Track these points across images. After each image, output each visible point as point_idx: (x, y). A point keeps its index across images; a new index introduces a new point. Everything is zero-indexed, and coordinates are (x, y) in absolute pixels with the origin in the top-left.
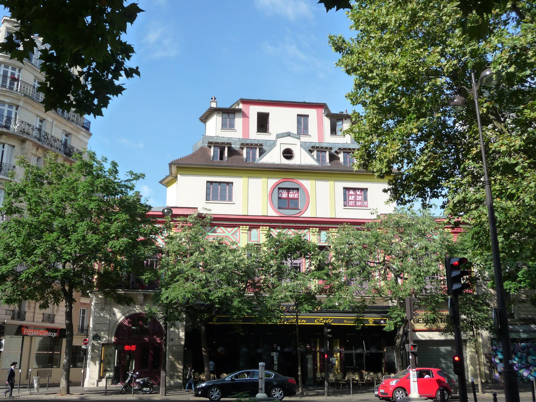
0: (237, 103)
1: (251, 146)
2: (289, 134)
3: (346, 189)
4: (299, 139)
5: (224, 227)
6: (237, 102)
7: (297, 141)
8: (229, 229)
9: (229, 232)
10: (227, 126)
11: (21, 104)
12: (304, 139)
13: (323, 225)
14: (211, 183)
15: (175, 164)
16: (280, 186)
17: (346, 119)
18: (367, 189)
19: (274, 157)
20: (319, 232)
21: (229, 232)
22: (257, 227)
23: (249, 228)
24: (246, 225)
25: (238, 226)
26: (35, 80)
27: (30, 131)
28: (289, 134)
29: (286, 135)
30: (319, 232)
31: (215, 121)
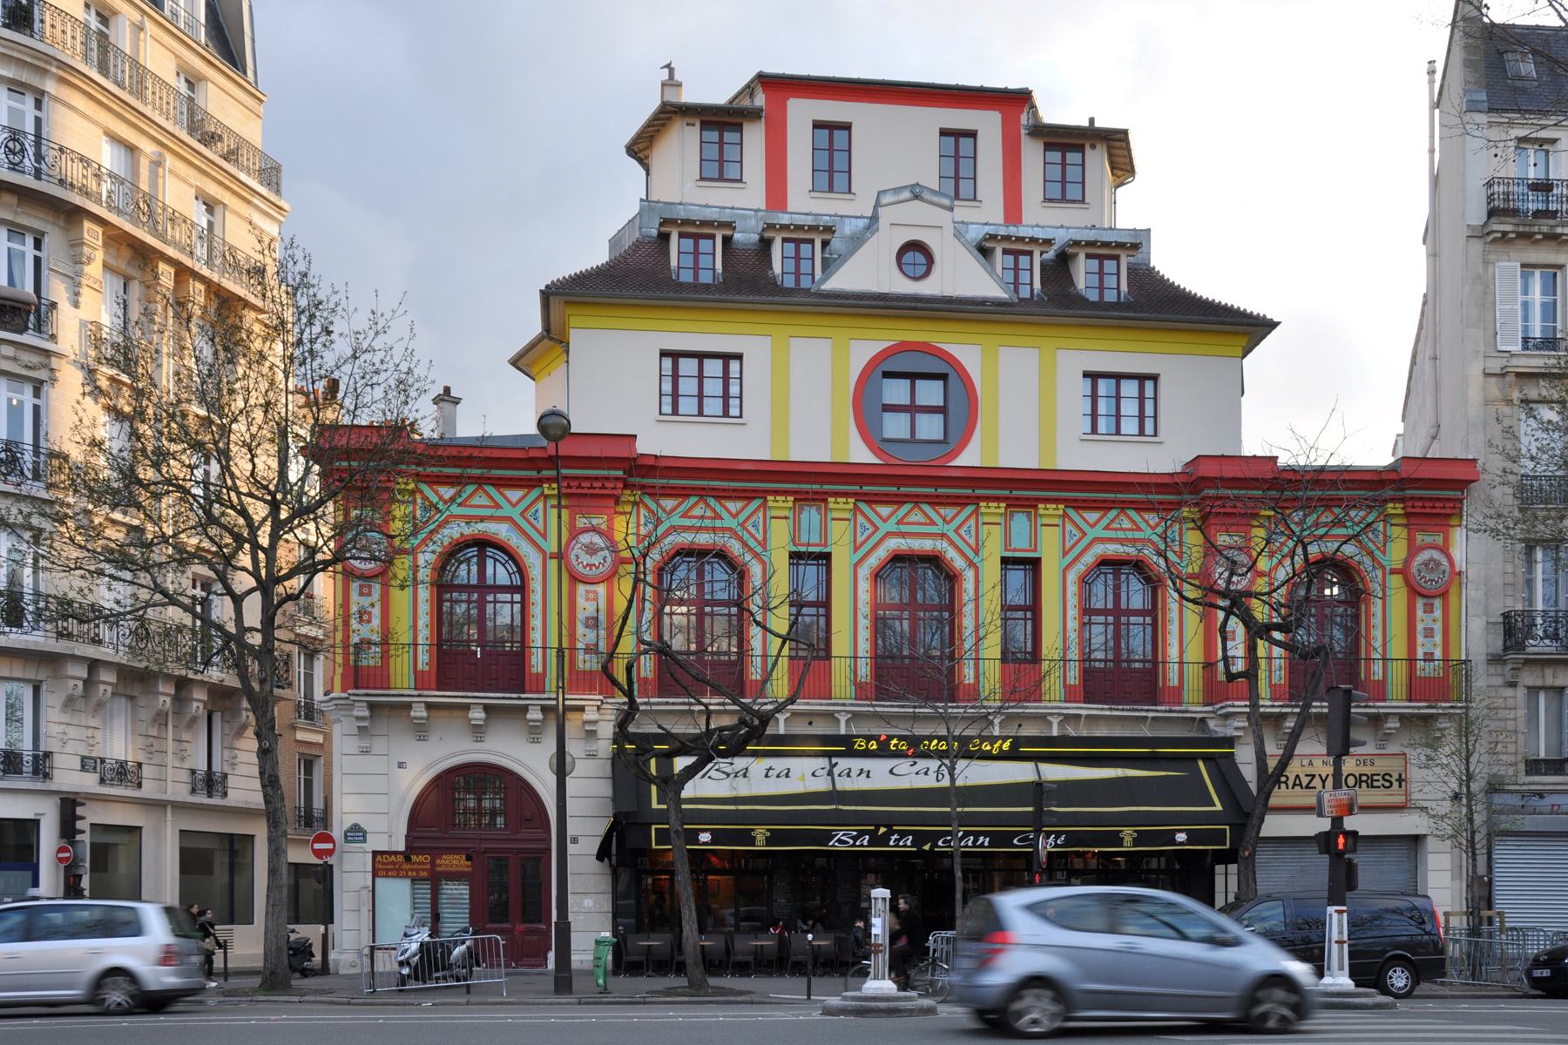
0: (749, 90)
1: (799, 235)
2: (917, 193)
3: (1093, 376)
4: (951, 209)
5: (717, 498)
6: (748, 86)
7: (943, 217)
10: (719, 170)
12: (963, 212)
13: (1023, 490)
14: (675, 355)
15: (557, 294)
16: (889, 366)
19: (869, 270)
20: (1008, 517)
21: (735, 516)
23: (796, 500)
24: (785, 493)
25: (762, 494)
26: (87, 6)
27: (92, 184)
28: (917, 193)
29: (906, 194)
30: (1008, 517)
31: (683, 144)
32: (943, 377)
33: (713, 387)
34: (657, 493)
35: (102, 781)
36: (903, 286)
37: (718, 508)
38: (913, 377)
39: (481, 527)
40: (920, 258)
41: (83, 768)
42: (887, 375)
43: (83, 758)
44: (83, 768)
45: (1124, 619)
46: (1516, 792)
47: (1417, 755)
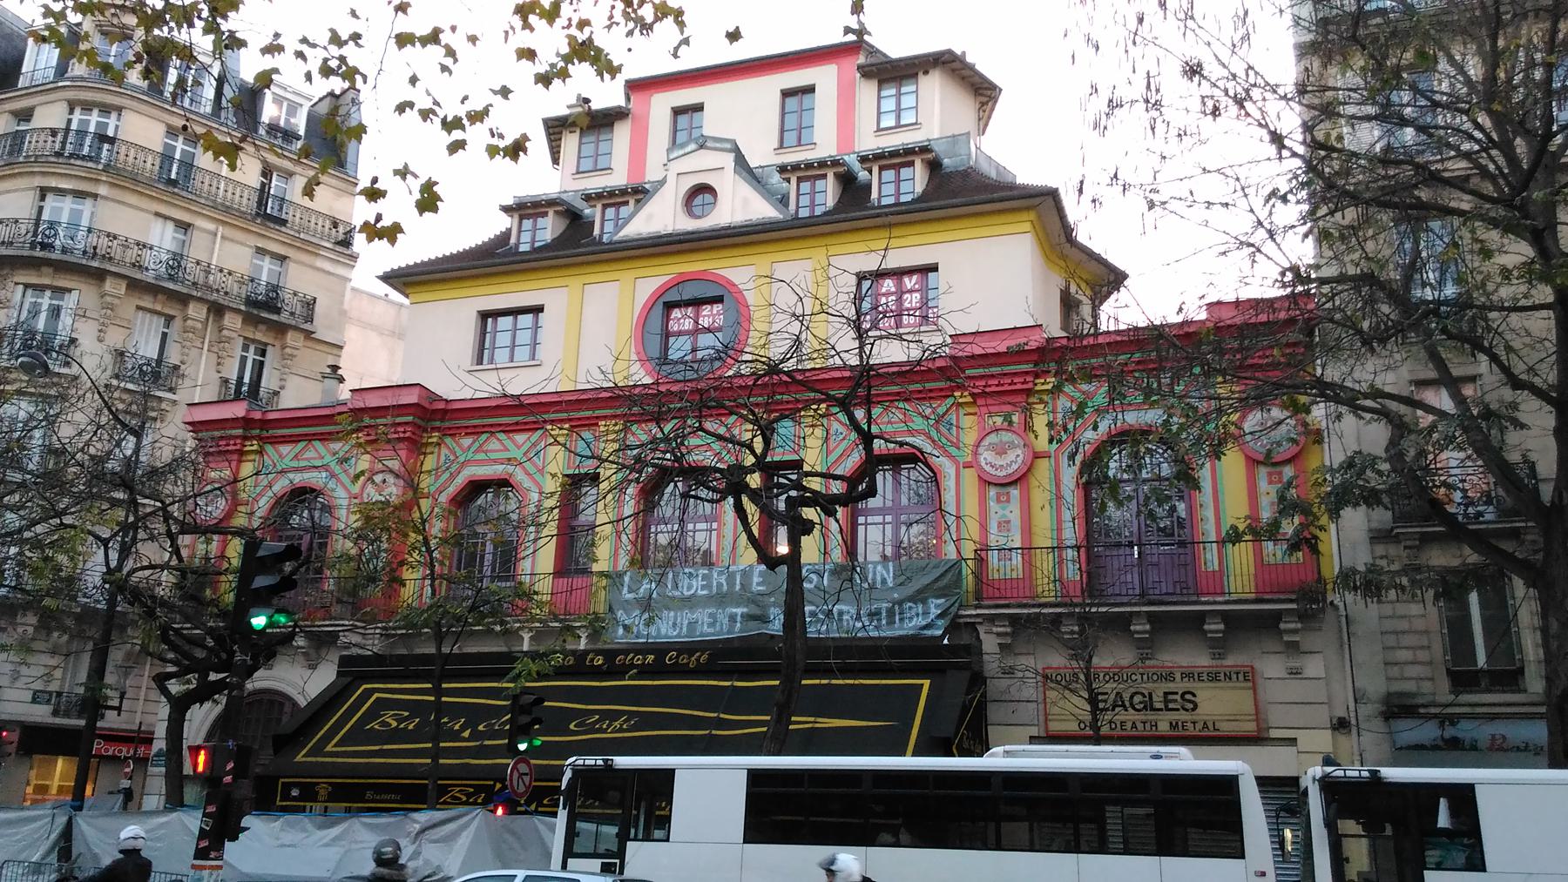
8: (520, 438)
9: (519, 447)
11: (103, 190)
16: (673, 296)
17: (926, 73)
18: (934, 268)
19: (661, 216)
22: (591, 423)
32: (718, 300)
33: (524, 337)
34: (453, 433)
35: (55, 713)
36: (688, 224)
37: (508, 443)
38: (697, 303)
39: (306, 475)
40: (708, 197)
41: (34, 701)
42: (670, 306)
43: (35, 692)
44: (34, 701)
45: (889, 518)
46: (1435, 716)
47: (1271, 667)
